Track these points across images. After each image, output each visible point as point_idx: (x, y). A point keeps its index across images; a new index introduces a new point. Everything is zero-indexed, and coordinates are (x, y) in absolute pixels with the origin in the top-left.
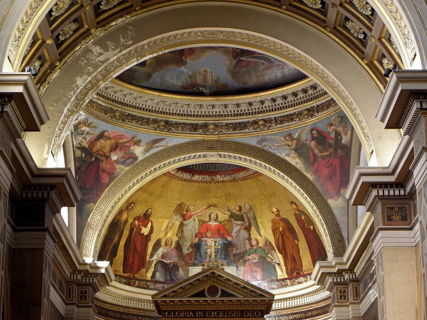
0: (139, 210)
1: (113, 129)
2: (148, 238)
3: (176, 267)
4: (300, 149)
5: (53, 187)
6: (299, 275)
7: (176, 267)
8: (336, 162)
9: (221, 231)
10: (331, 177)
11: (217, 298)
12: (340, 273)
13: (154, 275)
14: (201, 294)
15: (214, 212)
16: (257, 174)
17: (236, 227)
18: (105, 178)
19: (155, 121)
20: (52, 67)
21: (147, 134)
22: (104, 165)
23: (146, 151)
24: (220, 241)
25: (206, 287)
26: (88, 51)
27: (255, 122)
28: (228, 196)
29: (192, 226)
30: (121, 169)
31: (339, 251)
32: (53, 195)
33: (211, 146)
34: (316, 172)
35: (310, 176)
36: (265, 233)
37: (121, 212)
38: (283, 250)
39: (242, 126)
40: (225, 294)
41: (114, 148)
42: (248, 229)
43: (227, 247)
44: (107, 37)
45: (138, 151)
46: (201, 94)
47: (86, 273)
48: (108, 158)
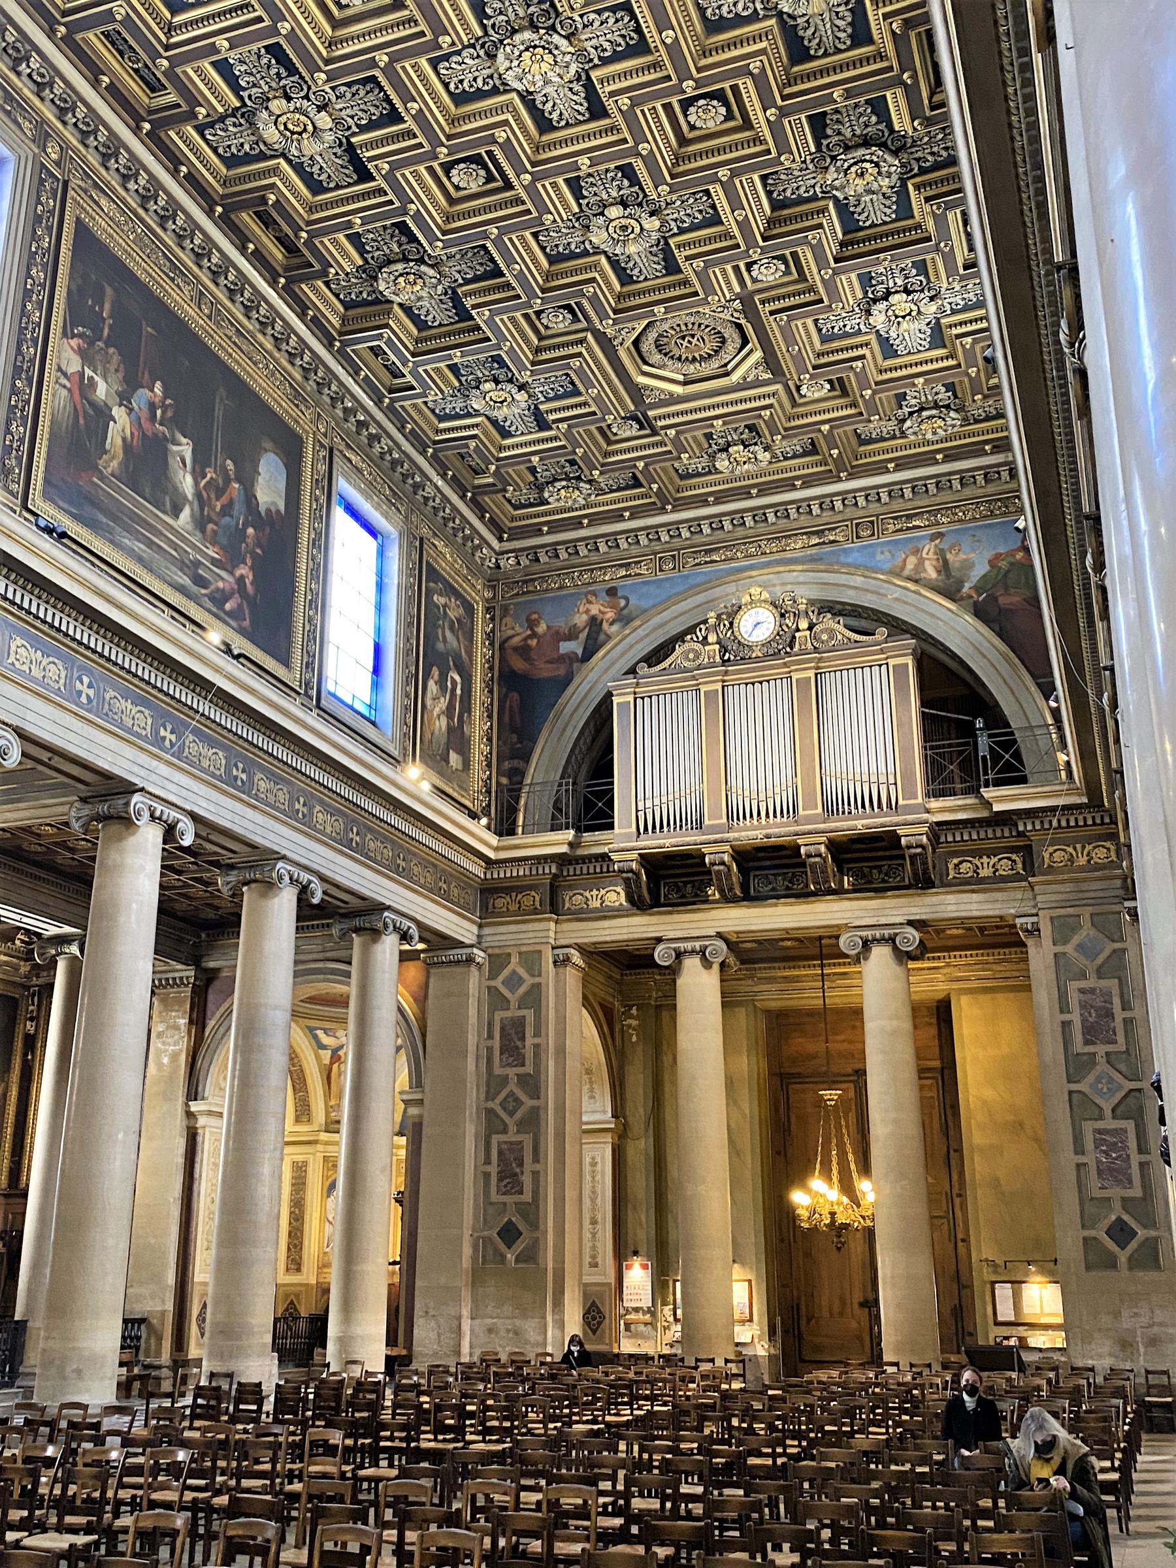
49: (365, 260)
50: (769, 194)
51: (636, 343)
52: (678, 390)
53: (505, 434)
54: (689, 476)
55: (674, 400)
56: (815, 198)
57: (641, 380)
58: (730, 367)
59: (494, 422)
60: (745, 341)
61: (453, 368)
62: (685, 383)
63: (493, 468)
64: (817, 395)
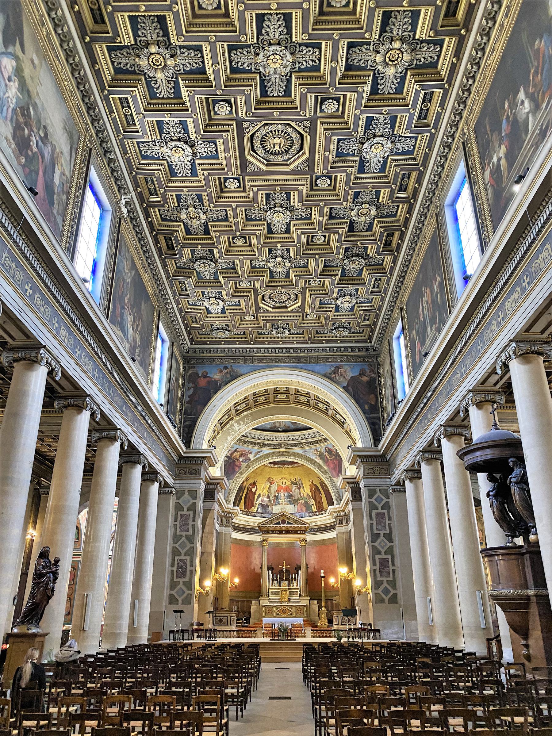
0: (251, 481)
1: (241, 447)
2: (255, 493)
3: (267, 506)
4: (321, 456)
5: (218, 483)
6: (322, 510)
7: (267, 506)
8: (337, 462)
9: (287, 489)
10: (334, 469)
11: (285, 525)
12: (339, 512)
13: (257, 510)
14: (278, 523)
15: (284, 480)
16: (303, 465)
17: (294, 487)
18: (237, 469)
19: (259, 443)
20: (218, 433)
21: (255, 449)
22: (237, 463)
23: (255, 456)
24: (287, 494)
25: (280, 520)
26: (232, 425)
27: (302, 443)
28: (290, 474)
29: (274, 487)
30: (244, 465)
31: (339, 503)
32: (218, 486)
33: (282, 455)
34: (328, 466)
35: (326, 468)
36: (307, 491)
37: (243, 482)
38: (314, 499)
39: (296, 445)
40: (288, 523)
41: (240, 456)
42: (299, 489)
43: (290, 496)
44: (240, 420)
45: (251, 456)
46: (278, 431)
47: (229, 513)
48: (238, 460)
49: (135, 40)
50: (347, 59)
51: (252, 137)
52: (264, 168)
53: (173, 173)
54: (251, 220)
55: (260, 172)
56: (365, 69)
57: (249, 157)
58: (289, 162)
59: (170, 166)
60: (301, 148)
61: (160, 124)
62: (267, 165)
63: (162, 190)
64: (323, 186)
